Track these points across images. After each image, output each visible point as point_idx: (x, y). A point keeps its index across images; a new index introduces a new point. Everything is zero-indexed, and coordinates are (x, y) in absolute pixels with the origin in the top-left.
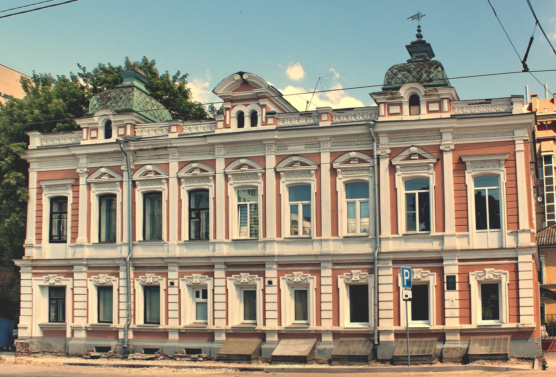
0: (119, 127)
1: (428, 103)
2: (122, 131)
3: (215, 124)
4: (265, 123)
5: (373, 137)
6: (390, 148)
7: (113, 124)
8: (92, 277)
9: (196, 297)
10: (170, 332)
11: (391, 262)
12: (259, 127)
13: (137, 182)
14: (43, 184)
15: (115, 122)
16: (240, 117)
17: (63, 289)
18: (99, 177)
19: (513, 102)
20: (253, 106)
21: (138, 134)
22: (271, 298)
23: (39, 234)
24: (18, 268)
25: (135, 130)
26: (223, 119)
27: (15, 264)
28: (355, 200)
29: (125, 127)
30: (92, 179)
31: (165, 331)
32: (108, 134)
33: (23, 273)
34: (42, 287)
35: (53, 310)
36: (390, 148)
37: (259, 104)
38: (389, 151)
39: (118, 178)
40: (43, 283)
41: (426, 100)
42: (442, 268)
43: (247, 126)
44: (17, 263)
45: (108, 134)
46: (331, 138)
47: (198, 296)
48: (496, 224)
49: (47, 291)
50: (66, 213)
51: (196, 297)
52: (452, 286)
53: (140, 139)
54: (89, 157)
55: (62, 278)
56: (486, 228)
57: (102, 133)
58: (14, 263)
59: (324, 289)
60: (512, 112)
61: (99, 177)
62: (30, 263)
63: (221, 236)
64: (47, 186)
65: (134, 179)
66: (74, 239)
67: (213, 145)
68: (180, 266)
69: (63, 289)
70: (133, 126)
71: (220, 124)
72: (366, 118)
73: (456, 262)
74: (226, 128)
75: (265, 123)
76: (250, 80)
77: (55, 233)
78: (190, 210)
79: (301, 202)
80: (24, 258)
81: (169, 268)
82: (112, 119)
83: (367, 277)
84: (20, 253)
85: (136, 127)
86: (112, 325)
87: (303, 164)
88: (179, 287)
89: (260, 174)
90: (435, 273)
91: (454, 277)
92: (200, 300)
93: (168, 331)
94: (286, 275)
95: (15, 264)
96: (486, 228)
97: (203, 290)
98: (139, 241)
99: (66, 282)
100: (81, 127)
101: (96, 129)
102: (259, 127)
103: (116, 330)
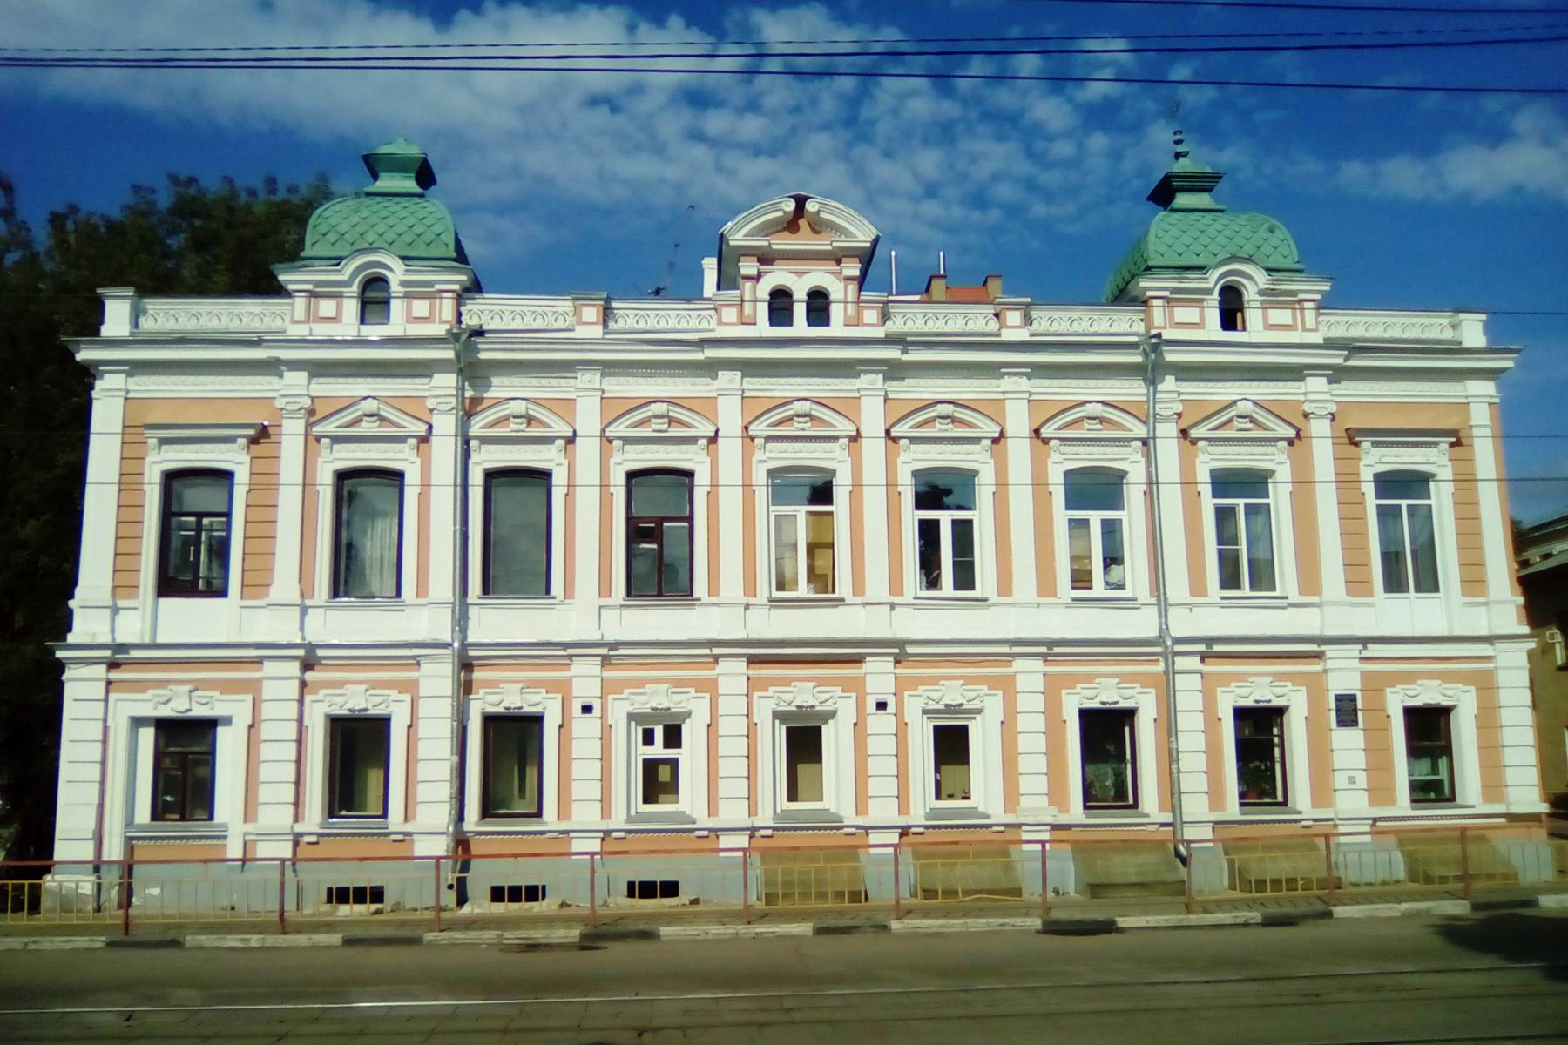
4: (858, 322)
12: (836, 328)
13: (473, 443)
16: (780, 304)
20: (819, 277)
34: (138, 722)
43: (800, 326)
48: (1428, 581)
55: (216, 694)
56: (1408, 591)
59: (1023, 723)
90: (1304, 688)
91: (1353, 698)
92: (658, 750)
96: (1408, 591)
102: (836, 328)
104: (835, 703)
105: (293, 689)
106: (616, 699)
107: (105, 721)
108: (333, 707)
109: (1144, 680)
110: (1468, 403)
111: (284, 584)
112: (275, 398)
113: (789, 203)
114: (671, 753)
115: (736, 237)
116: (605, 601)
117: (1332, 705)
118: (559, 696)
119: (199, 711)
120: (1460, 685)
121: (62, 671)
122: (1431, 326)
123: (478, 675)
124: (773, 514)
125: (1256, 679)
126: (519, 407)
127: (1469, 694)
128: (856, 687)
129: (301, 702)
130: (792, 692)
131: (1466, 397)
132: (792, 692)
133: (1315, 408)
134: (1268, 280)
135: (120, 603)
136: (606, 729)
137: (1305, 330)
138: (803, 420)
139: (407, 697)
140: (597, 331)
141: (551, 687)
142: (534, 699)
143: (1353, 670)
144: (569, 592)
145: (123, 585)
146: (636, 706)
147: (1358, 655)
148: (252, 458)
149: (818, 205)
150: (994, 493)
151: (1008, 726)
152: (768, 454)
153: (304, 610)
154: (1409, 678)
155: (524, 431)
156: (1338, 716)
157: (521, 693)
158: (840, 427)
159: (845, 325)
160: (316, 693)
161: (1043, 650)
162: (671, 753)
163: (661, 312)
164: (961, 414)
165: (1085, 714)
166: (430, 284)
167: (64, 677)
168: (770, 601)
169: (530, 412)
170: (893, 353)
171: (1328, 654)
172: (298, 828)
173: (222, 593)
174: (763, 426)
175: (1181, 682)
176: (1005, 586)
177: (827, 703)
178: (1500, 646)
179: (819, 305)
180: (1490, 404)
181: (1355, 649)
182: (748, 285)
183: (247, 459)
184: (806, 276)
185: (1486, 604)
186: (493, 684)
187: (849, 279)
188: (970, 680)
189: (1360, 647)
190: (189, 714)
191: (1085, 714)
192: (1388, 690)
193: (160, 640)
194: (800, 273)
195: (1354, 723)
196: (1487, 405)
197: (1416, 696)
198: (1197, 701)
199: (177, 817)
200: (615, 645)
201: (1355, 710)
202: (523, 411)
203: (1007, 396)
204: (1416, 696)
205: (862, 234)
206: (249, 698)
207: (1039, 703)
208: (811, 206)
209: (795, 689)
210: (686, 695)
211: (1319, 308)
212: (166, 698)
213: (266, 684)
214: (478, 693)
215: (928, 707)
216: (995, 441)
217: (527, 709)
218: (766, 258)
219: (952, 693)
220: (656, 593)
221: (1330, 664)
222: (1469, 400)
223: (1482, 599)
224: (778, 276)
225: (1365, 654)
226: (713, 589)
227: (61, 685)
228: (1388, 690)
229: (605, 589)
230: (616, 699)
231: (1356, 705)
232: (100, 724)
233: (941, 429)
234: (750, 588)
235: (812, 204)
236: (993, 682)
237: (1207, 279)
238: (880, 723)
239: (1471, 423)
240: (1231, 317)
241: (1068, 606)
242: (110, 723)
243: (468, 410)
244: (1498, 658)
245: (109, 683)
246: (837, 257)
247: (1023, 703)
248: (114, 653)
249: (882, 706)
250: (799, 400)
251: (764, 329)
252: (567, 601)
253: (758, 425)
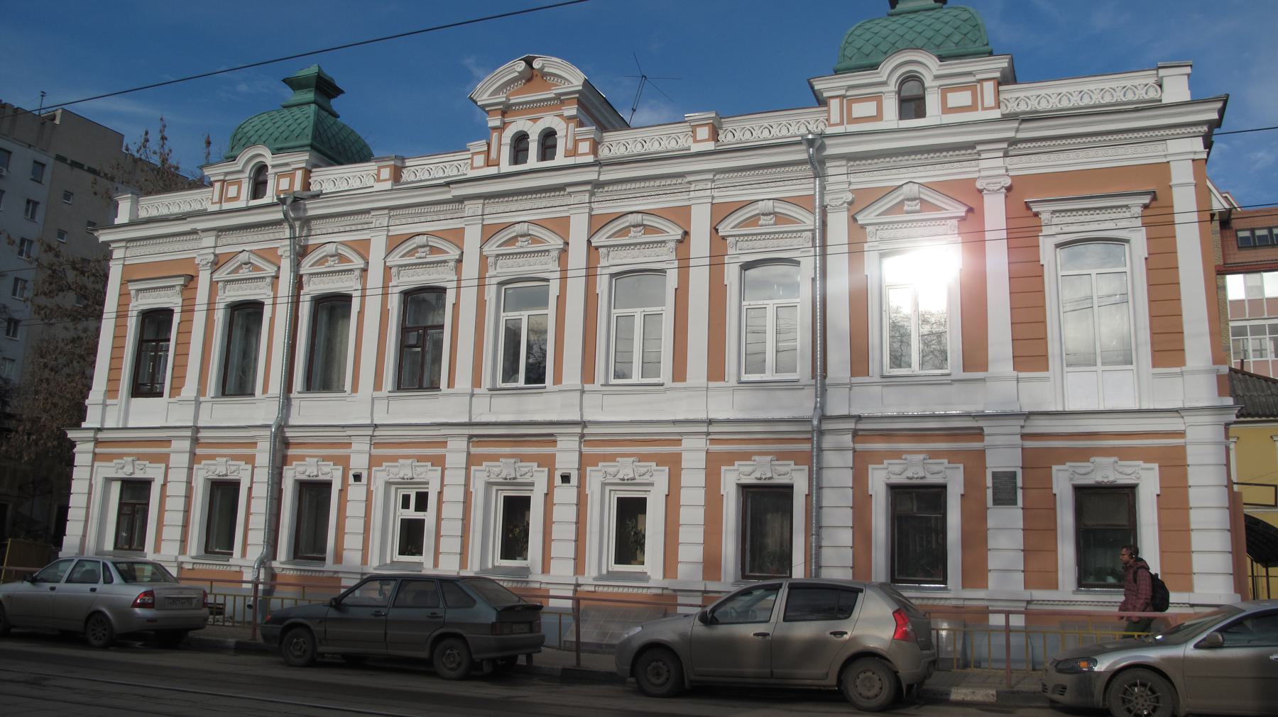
0: (279, 176)
1: (945, 90)
2: (284, 183)
3: (469, 161)
5: (818, 165)
6: (852, 191)
7: (270, 170)
8: (203, 462)
9: (403, 508)
10: (344, 578)
11: (849, 437)
12: (560, 159)
13: (304, 279)
14: (132, 287)
15: (273, 166)
17: (145, 484)
18: (236, 270)
19: (1162, 77)
20: (550, 120)
21: (315, 188)
22: (565, 513)
23: (113, 380)
24: (73, 444)
25: (310, 180)
26: (486, 148)
27: (68, 436)
28: (766, 302)
29: (291, 175)
30: (221, 275)
31: (336, 575)
32: (258, 188)
33: (78, 452)
34: (108, 481)
35: (124, 525)
36: (852, 191)
37: (561, 116)
38: (849, 197)
39: (270, 270)
40: (114, 470)
41: (941, 86)
42: (981, 454)
43: (533, 161)
44: (72, 435)
45: (258, 188)
46: (714, 176)
47: (406, 505)
49: (116, 489)
50: (169, 340)
51: (403, 508)
52: (1004, 495)
53: (318, 195)
54: (220, 233)
55: (146, 463)
57: (246, 188)
58: (66, 435)
60: (1161, 101)
61: (236, 270)
62: (91, 434)
63: (464, 380)
64: (138, 291)
65: (301, 273)
66: (176, 390)
67: (461, 200)
68: (375, 443)
69: (145, 484)
70: (307, 173)
71: (479, 160)
72: (796, 131)
73: (1017, 439)
74: (488, 166)
75: (573, 152)
76: (546, 70)
77: (144, 379)
78: (404, 330)
79: (642, 309)
80: (84, 425)
81: (354, 446)
82: (269, 159)
83: (792, 470)
84: (79, 414)
85: (311, 175)
86: (232, 561)
87: (648, 229)
88: (369, 484)
89: (555, 254)
91: (1013, 475)
92: (411, 513)
93: (340, 575)
94: (600, 464)
95: (68, 436)
97: (417, 493)
98: (299, 393)
99: (153, 472)
100: (212, 179)
101: (238, 183)
103: (238, 569)
104: (532, 476)
105: (186, 457)
106: (377, 471)
107: (91, 479)
108: (210, 473)
109: (798, 458)
110: (1168, 162)
111: (190, 388)
112: (195, 257)
113: (520, 65)
114: (419, 515)
115: (483, 98)
116: (377, 394)
117: (989, 482)
118: (341, 467)
119: (139, 475)
120: (1141, 463)
121: (75, 446)
122: (1135, 86)
123: (291, 452)
124: (505, 319)
125: (909, 457)
126: (330, 249)
127: (1151, 472)
128: (548, 462)
129: (190, 469)
130: (500, 466)
131: (1165, 156)
132: (500, 466)
133: (988, 184)
134: (940, 66)
135: (109, 402)
136: (369, 493)
137: (984, 109)
138: (524, 239)
139: (249, 467)
140: (388, 185)
141: (337, 460)
142: (326, 469)
143: (1013, 446)
144: (355, 388)
145: (112, 392)
146: (391, 476)
147: (1018, 430)
148: (183, 300)
149: (541, 62)
150: (676, 289)
151: (672, 500)
152: (499, 270)
153: (198, 403)
154: (1084, 455)
155: (333, 266)
156: (994, 494)
157: (318, 465)
158: (552, 242)
159: (565, 157)
160: (200, 463)
161: (704, 429)
162: (419, 515)
163: (424, 166)
164: (649, 221)
165: (744, 489)
166: (287, 164)
167: (75, 450)
168: (490, 390)
169: (339, 251)
170: (591, 175)
171: (986, 431)
172: (181, 558)
173: (161, 395)
174: (494, 248)
175: (831, 458)
176: (679, 373)
177: (526, 476)
178: (1189, 419)
179: (548, 141)
180: (1193, 160)
181: (1015, 426)
182: (495, 135)
183: (179, 300)
184: (539, 121)
185: (1182, 373)
186: (302, 458)
187: (570, 118)
188: (643, 458)
189: (1022, 423)
190: (133, 476)
191: (744, 489)
192: (1055, 468)
193: (129, 426)
194: (534, 120)
195: (1014, 502)
196: (1191, 161)
197: (1088, 473)
198: (847, 478)
199: (127, 547)
200: (376, 426)
201: (1015, 488)
202: (333, 251)
203: (692, 202)
204: (1088, 473)
205: (574, 79)
206: (163, 466)
207: (700, 479)
208: (537, 64)
209: (501, 464)
210: (425, 468)
211: (999, 84)
212: (122, 465)
213: (172, 457)
214: (291, 465)
215: (491, 480)
216: (679, 242)
217: (321, 478)
218: (506, 110)
219: (626, 468)
220: (417, 387)
221: (988, 440)
222: (1169, 159)
223: (1177, 370)
224: (520, 124)
225: (1026, 431)
226: (451, 384)
227: (73, 455)
228: (1055, 468)
229: (378, 386)
230: (377, 471)
231: (1015, 483)
232: (88, 482)
233: (636, 236)
234: (477, 382)
235: (537, 63)
236: (660, 460)
237: (878, 73)
238: (566, 495)
239: (1171, 184)
240: (912, 105)
241: (734, 389)
242: (93, 482)
243: (301, 253)
244: (1187, 431)
245: (95, 454)
246: (560, 100)
247: (686, 479)
248: (96, 434)
249: (566, 479)
250: (519, 223)
251: (506, 167)
252: (353, 395)
253: (490, 247)
